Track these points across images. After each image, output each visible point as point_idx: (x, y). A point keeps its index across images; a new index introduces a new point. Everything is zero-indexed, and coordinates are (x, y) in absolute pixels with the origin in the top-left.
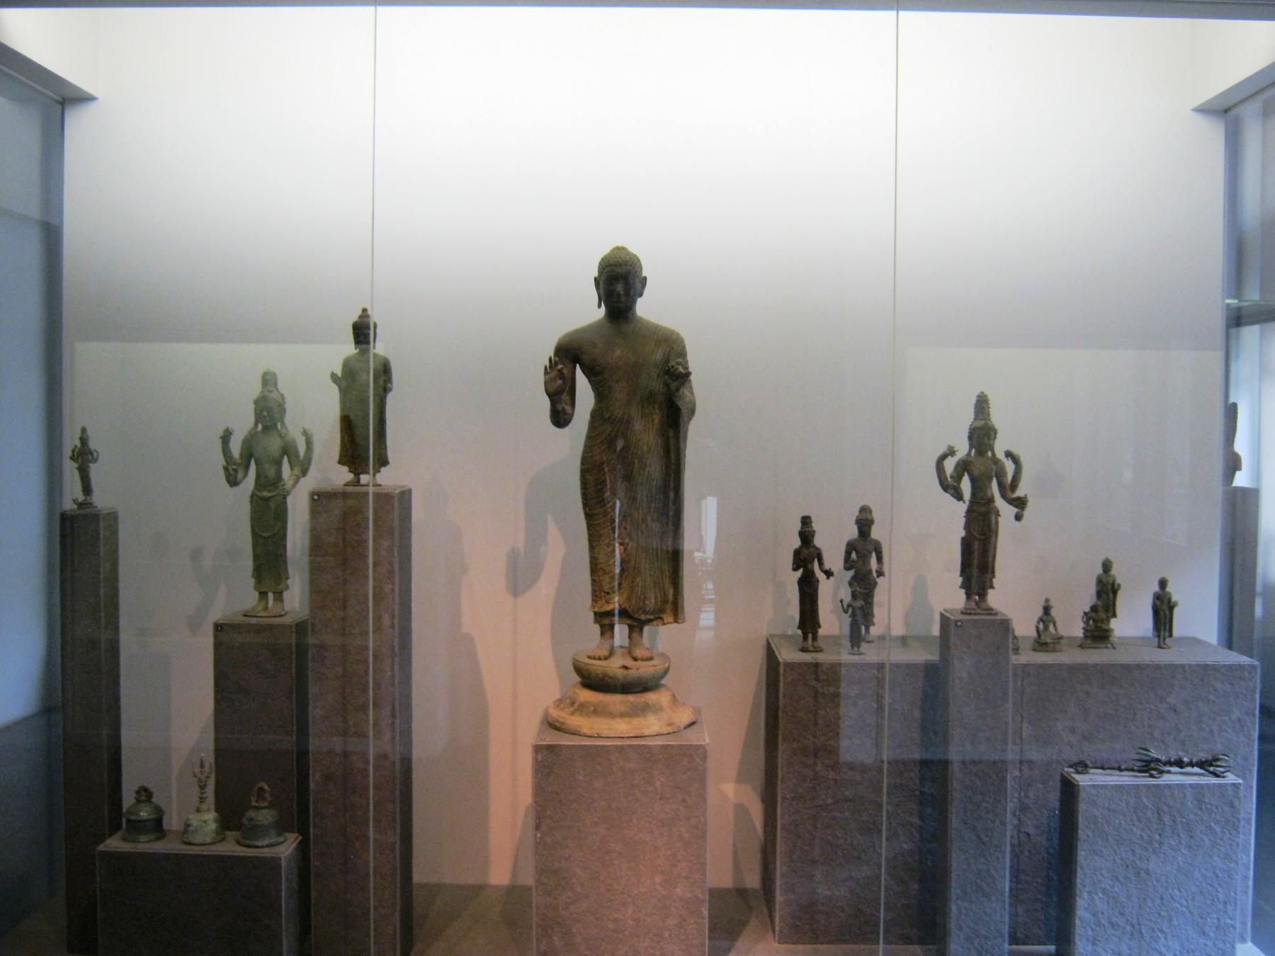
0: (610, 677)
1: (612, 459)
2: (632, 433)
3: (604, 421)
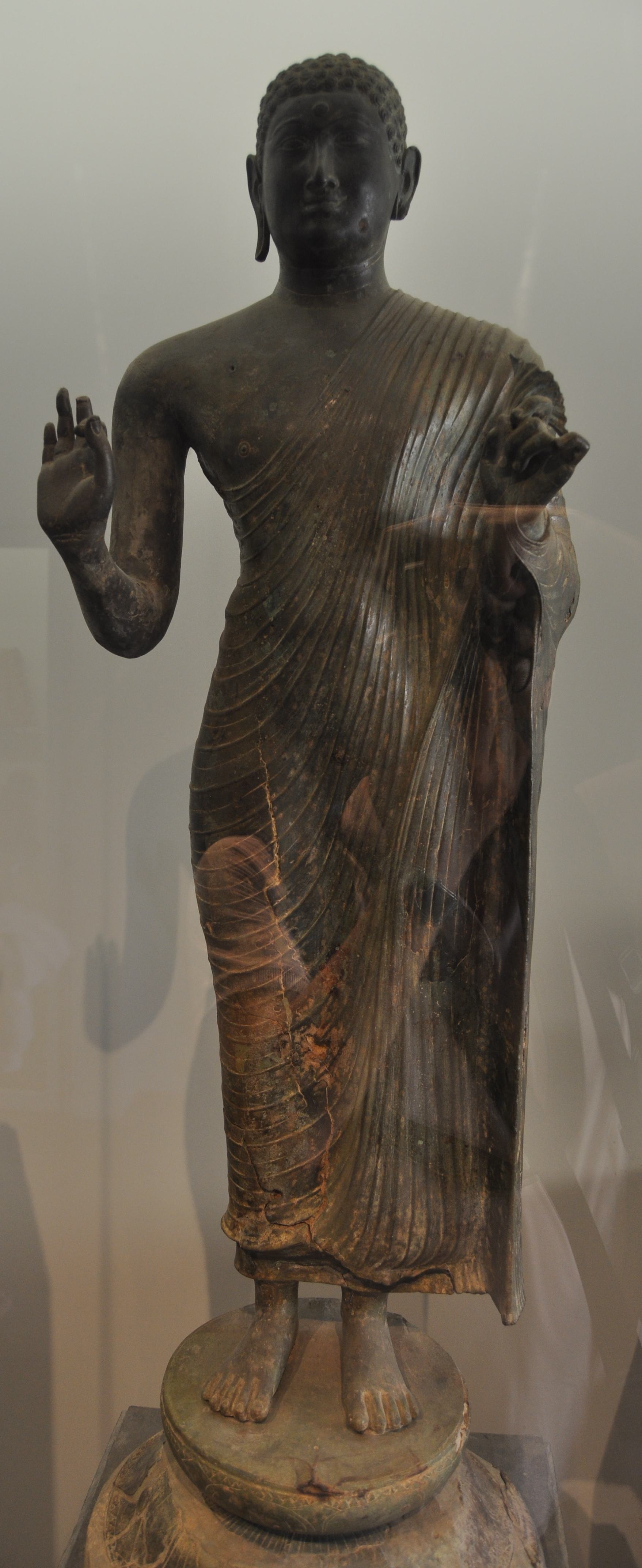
1: (292, 764)
2: (360, 676)
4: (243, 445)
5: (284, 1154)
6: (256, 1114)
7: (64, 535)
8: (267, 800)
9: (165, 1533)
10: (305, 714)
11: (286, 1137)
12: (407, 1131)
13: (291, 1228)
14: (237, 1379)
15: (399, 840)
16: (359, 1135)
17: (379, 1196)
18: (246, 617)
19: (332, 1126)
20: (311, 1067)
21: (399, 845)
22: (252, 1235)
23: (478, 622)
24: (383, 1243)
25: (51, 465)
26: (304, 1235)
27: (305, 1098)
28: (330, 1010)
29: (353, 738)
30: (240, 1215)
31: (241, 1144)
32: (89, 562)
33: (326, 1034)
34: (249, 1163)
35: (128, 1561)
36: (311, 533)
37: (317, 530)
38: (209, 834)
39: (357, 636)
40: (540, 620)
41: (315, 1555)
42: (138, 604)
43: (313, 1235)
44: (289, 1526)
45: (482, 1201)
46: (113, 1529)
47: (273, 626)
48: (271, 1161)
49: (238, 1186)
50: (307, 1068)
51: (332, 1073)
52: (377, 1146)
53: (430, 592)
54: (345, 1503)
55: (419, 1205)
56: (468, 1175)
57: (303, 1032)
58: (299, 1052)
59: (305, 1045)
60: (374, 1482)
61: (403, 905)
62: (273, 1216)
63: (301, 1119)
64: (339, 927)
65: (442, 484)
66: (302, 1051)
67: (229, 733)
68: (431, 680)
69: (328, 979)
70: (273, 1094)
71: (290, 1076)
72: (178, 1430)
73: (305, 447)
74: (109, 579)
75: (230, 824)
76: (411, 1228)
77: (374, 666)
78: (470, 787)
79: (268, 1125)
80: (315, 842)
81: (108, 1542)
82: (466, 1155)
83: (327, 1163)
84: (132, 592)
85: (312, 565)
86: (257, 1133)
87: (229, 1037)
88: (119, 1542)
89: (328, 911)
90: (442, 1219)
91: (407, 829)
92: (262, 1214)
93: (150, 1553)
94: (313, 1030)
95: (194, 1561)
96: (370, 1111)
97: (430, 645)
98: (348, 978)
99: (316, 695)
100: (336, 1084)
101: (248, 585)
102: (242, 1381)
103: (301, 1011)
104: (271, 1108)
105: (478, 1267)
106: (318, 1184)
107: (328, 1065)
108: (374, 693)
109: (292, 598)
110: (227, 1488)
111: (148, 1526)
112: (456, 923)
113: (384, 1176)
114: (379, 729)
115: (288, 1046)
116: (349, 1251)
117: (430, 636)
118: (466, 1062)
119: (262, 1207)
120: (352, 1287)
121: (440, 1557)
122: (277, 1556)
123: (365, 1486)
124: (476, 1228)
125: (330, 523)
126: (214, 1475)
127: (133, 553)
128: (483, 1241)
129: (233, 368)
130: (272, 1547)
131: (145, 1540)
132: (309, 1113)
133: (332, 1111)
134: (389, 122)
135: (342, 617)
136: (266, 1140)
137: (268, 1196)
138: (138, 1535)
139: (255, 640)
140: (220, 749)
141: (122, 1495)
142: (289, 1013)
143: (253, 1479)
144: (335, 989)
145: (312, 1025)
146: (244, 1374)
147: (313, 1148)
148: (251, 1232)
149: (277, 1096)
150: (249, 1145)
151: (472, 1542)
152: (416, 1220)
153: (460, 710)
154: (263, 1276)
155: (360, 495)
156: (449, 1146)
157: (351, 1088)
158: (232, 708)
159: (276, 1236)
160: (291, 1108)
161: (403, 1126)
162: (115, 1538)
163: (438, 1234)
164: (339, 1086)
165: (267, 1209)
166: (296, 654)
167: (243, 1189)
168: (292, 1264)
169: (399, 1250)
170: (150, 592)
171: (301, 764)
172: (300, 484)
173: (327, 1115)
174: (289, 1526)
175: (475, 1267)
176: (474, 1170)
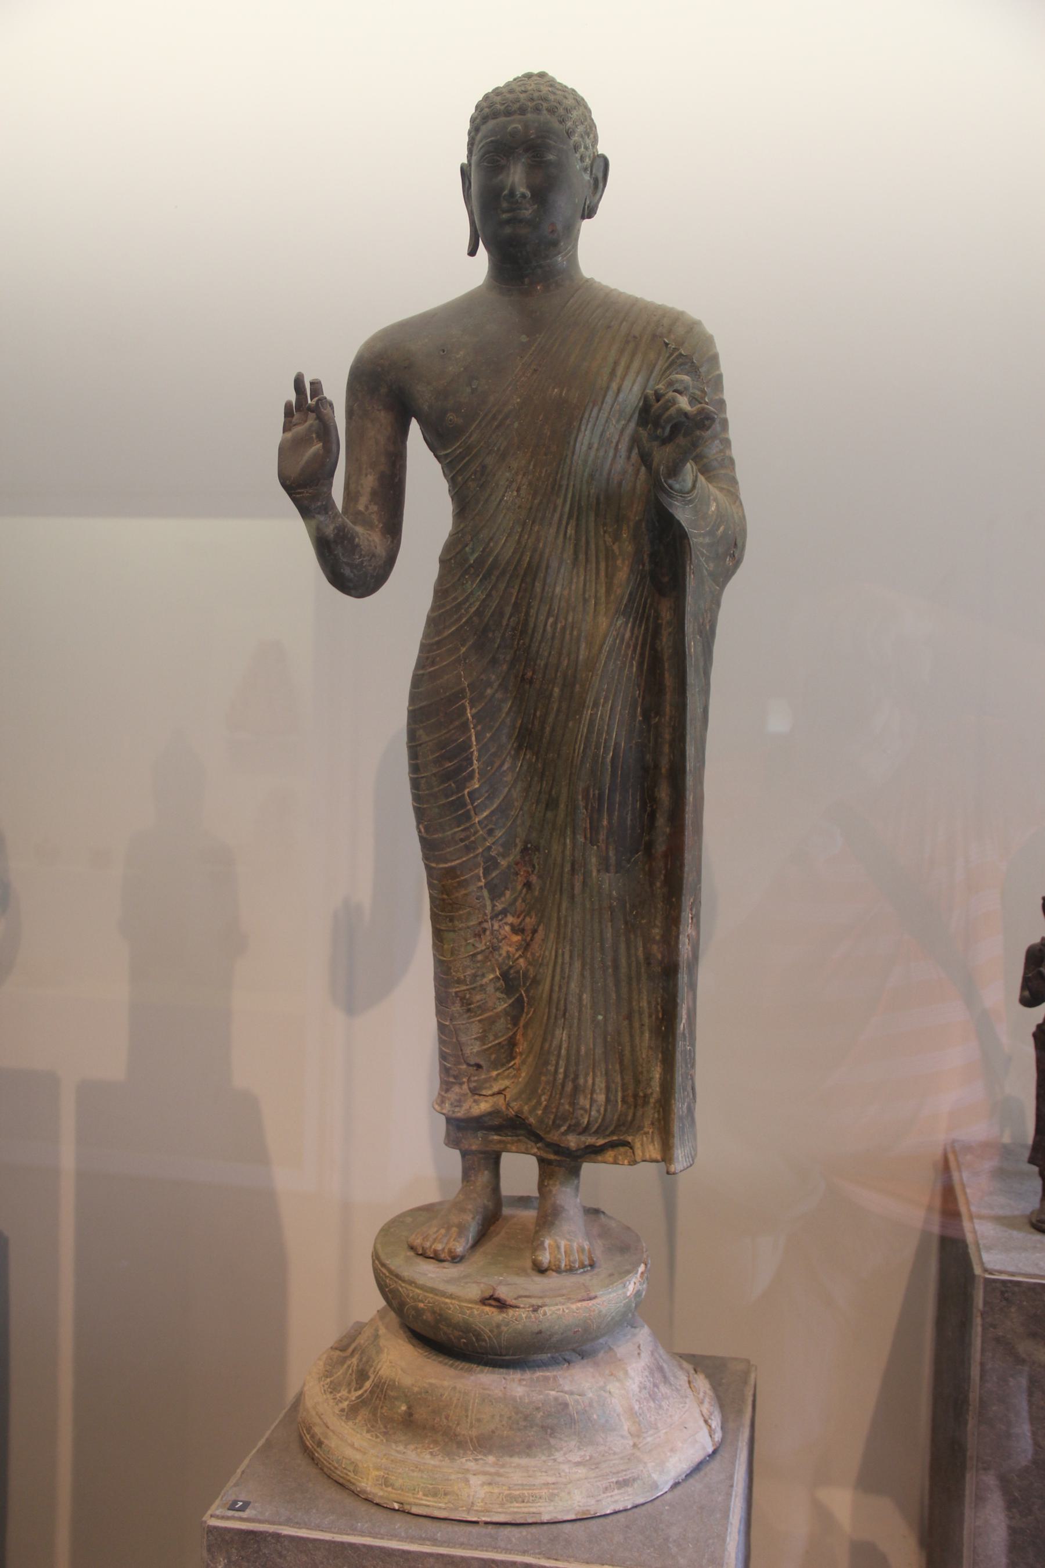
0: (456, 1326)
1: (489, 684)
2: (545, 609)
3: (466, 572)
4: (451, 416)
6: (460, 994)
7: (299, 491)
8: (467, 714)
9: (371, 1366)
11: (486, 1015)
12: (589, 1007)
13: (489, 1097)
15: (577, 747)
16: (547, 1010)
17: (564, 1064)
18: (453, 561)
19: (526, 1004)
20: (508, 952)
21: (577, 751)
24: (567, 1107)
25: (289, 435)
26: (500, 1103)
28: (524, 901)
29: (538, 661)
30: (447, 1091)
31: (447, 1023)
33: (520, 923)
34: (454, 1040)
35: (339, 1392)
37: (509, 487)
38: (420, 745)
39: (541, 575)
42: (361, 550)
43: (507, 1099)
45: (658, 1076)
47: (473, 567)
48: (473, 1037)
49: (445, 1063)
50: (504, 954)
51: (526, 958)
52: (563, 1020)
53: (609, 539)
55: (599, 1074)
56: (644, 1052)
57: (501, 920)
58: (497, 938)
59: (502, 932)
60: (547, 1301)
61: (582, 804)
62: (475, 1087)
63: (499, 999)
64: (530, 826)
65: (620, 447)
66: (500, 937)
69: (522, 873)
71: (490, 960)
72: (383, 1265)
74: (336, 528)
75: (437, 736)
76: (592, 1094)
79: (470, 1004)
80: (509, 753)
82: (642, 1033)
84: (357, 540)
85: (504, 516)
86: (461, 1011)
87: (438, 926)
88: (331, 1382)
89: (521, 813)
90: (619, 1088)
91: (584, 738)
92: (465, 1087)
93: (357, 1383)
94: (510, 919)
95: (394, 1381)
96: (556, 988)
97: (606, 583)
98: (539, 872)
99: (507, 625)
100: (529, 967)
101: (455, 534)
104: (474, 989)
106: (513, 1058)
107: (522, 950)
108: (555, 623)
110: (421, 1305)
111: (358, 1366)
112: (629, 822)
113: (568, 1047)
114: (560, 654)
115: (488, 933)
116: (537, 1114)
117: (607, 576)
118: (641, 949)
119: (465, 1080)
120: (545, 1155)
123: (539, 1302)
124: (652, 1100)
125: (519, 481)
126: (411, 1295)
128: (659, 1112)
129: (444, 351)
131: (354, 1376)
132: (506, 994)
133: (527, 991)
134: (576, 138)
135: (528, 559)
137: (472, 1070)
138: (348, 1375)
139: (459, 580)
140: (430, 672)
142: (488, 903)
143: (443, 1294)
144: (528, 881)
145: (508, 914)
147: (509, 1026)
148: (455, 1104)
149: (478, 978)
152: (596, 1087)
153: (631, 638)
154: (467, 1147)
155: (544, 457)
156: (626, 1023)
157: (541, 970)
158: (440, 638)
159: (478, 1105)
160: (490, 989)
161: (585, 1003)
162: (328, 1380)
163: (617, 1101)
165: (469, 1081)
166: (491, 590)
167: (449, 1065)
168: (492, 1135)
169: (582, 1115)
170: (374, 540)
171: (496, 685)
173: (521, 995)
175: (652, 1139)
176: (650, 1047)
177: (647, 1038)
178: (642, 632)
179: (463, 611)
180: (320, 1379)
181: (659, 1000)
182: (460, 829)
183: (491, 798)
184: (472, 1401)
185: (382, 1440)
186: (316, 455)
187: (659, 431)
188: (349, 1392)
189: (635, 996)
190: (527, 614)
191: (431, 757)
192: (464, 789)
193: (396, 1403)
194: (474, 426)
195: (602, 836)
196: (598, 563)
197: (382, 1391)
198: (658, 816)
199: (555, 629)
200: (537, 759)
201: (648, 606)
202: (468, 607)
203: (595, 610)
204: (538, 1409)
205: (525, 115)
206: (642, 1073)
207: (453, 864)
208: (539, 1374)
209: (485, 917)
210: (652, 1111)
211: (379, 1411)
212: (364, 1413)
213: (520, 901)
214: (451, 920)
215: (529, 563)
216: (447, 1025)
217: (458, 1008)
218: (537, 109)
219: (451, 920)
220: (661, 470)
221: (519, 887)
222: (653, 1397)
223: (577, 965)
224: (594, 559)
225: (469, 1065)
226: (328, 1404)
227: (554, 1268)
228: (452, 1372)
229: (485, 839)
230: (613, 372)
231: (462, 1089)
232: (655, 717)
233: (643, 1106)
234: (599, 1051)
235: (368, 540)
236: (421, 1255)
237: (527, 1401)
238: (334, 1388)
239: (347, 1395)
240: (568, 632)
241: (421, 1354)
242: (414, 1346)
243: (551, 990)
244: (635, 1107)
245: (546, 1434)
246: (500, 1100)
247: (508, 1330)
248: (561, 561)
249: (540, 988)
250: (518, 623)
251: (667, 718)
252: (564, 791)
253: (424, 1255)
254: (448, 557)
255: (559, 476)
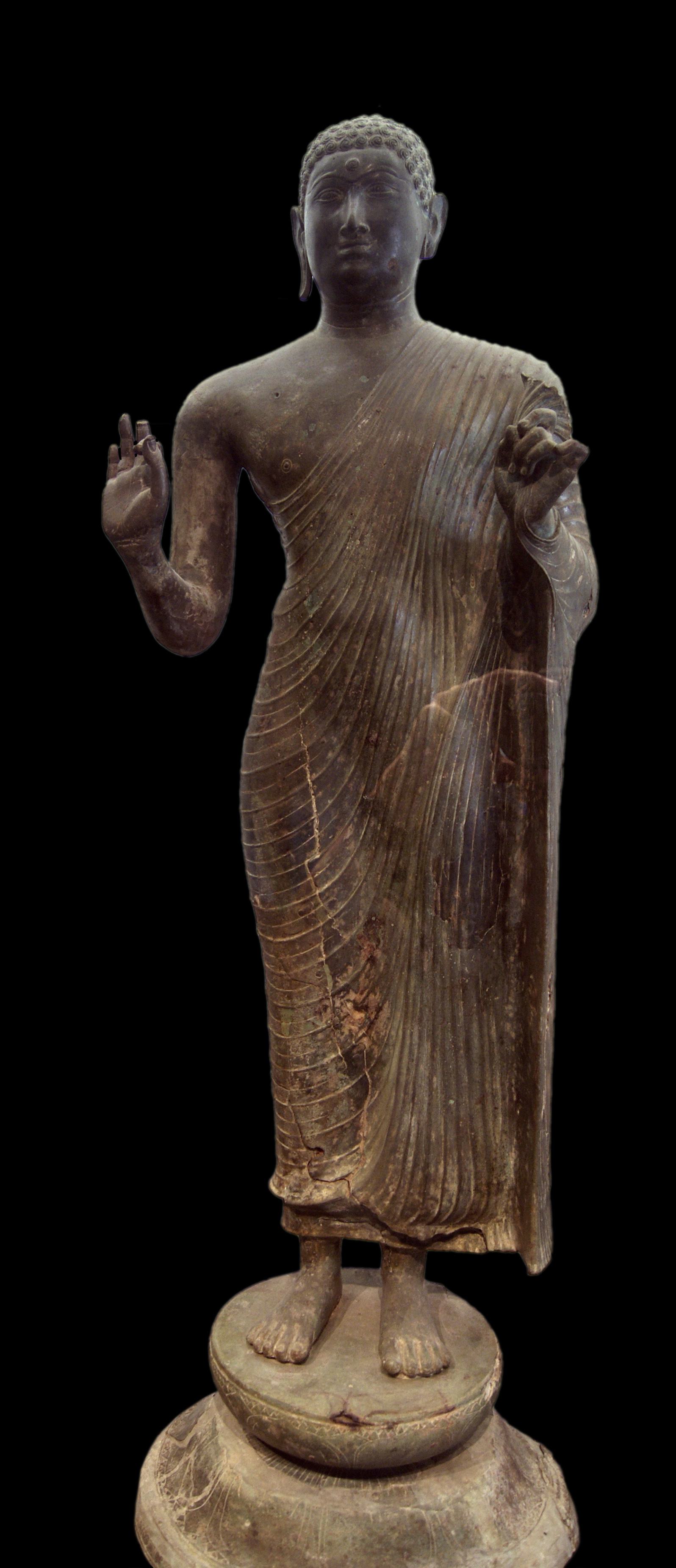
0: (303, 1443)
1: (331, 747)
2: (392, 665)
3: (305, 627)
5: (326, 1113)
7: (126, 540)
8: (307, 779)
9: (210, 1469)
10: (341, 701)
11: (327, 1097)
12: (439, 1091)
13: (332, 1183)
14: (279, 1326)
15: (427, 814)
17: (413, 1152)
18: (289, 616)
20: (350, 1030)
21: (427, 820)
22: (296, 1191)
23: (500, 617)
24: (417, 1197)
26: (344, 1191)
27: (346, 1060)
28: (367, 977)
29: (384, 723)
32: (146, 565)
33: (364, 1000)
34: (293, 1122)
35: (176, 1495)
36: (345, 538)
37: (352, 535)
38: (257, 812)
39: (388, 630)
40: (553, 612)
41: (348, 1490)
42: (192, 605)
43: (351, 1189)
44: (323, 1456)
45: (512, 1162)
46: (163, 1469)
47: (312, 622)
48: (314, 1120)
49: (283, 1145)
50: (347, 1032)
51: (370, 1037)
52: (411, 1104)
53: (456, 591)
54: (374, 1434)
55: (451, 1162)
56: (498, 1137)
57: (342, 997)
58: (339, 1016)
59: (344, 1009)
61: (432, 876)
62: (316, 1173)
63: (341, 1080)
64: (375, 898)
67: (274, 720)
68: (456, 670)
69: (365, 948)
70: (315, 1057)
71: (331, 1039)
73: (340, 462)
74: (165, 581)
77: (403, 657)
78: (493, 767)
79: (310, 1086)
80: (352, 820)
81: (158, 1480)
82: (495, 1117)
83: (365, 1122)
84: (187, 594)
85: (347, 567)
87: (275, 1002)
88: (168, 1479)
89: (364, 884)
90: (472, 1177)
92: (305, 1171)
93: (195, 1487)
94: (352, 996)
96: (404, 1071)
97: (456, 638)
98: (384, 946)
99: (350, 684)
100: (373, 1046)
101: (292, 587)
102: (284, 1327)
103: (341, 977)
104: (314, 1069)
105: (509, 1227)
106: (358, 1143)
107: (366, 1029)
108: (403, 681)
109: (329, 596)
110: (265, 1418)
111: (195, 1464)
112: (482, 894)
113: (418, 1133)
114: (408, 714)
115: (329, 1010)
116: (384, 1205)
117: (456, 630)
118: (494, 1027)
119: (305, 1164)
121: (469, 1500)
122: (313, 1488)
123: (394, 1418)
124: (506, 1188)
125: (362, 528)
126: (254, 1406)
127: (190, 561)
128: (513, 1200)
129: (277, 395)
130: (308, 1481)
132: (349, 1075)
133: (371, 1072)
134: (416, 174)
135: (373, 612)
136: (310, 1100)
137: (313, 1154)
138: (186, 1473)
139: (297, 636)
140: (265, 735)
141: (173, 1441)
142: (329, 979)
143: (289, 1409)
146: (287, 1321)
147: (352, 1108)
148: (295, 1189)
149: (319, 1058)
150: (294, 1105)
151: (502, 1492)
152: (448, 1176)
153: (484, 697)
156: (479, 1106)
157: (387, 1051)
158: (276, 698)
159: (319, 1191)
160: (332, 1069)
161: (435, 1086)
162: (165, 1476)
163: (469, 1191)
164: (376, 1049)
167: (287, 1148)
169: (432, 1205)
170: (204, 596)
171: (338, 748)
172: (336, 495)
173: (365, 1076)
174: (323, 1456)
175: (506, 1227)
176: (504, 1132)
177: (501, 1122)
178: (495, 689)
179: (301, 669)
180: (156, 1473)
181: (513, 1081)
182: (299, 901)
183: (332, 869)
184: (321, 1521)
185: (226, 1562)
186: (144, 500)
187: (523, 470)
188: (187, 1495)
189: (488, 1076)
190: (373, 671)
191: (268, 826)
192: (303, 861)
193: (239, 1518)
194: (312, 471)
195: (454, 910)
196: (446, 616)
197: (223, 1501)
198: (511, 885)
199: (403, 688)
200: (383, 825)
201: (500, 661)
202: (307, 665)
203: (445, 667)
204: (393, 1529)
205: (363, 148)
206: (495, 1159)
207: (292, 938)
208: (392, 1486)
209: (326, 995)
210: (506, 1199)
211: (221, 1524)
212: (204, 1526)
213: (363, 976)
214: (290, 997)
215: (375, 616)
216: (285, 1106)
217: (297, 1089)
218: (376, 144)
219: (290, 997)
220: (525, 511)
221: (363, 962)
222: (510, 1501)
223: (427, 1046)
224: (442, 613)
225: (309, 1148)
226: (166, 1509)
227: (406, 1372)
228: (299, 1485)
229: (326, 913)
230: (461, 414)
231: (301, 1173)
232: (510, 781)
233: (496, 1195)
234: (452, 1136)
235: (199, 595)
236: (262, 1354)
237: (381, 1520)
238: (170, 1488)
239: (185, 1499)
240: (417, 691)
241: (264, 1460)
242: (255, 1448)
243: (399, 1073)
244: (489, 1194)
245: (403, 1557)
246: (344, 1190)
247: (361, 1449)
248: (408, 614)
249: (386, 1069)
250: (362, 682)
251: (522, 781)
252: (413, 862)
253: (265, 1354)
254: (285, 612)
255: (405, 522)
